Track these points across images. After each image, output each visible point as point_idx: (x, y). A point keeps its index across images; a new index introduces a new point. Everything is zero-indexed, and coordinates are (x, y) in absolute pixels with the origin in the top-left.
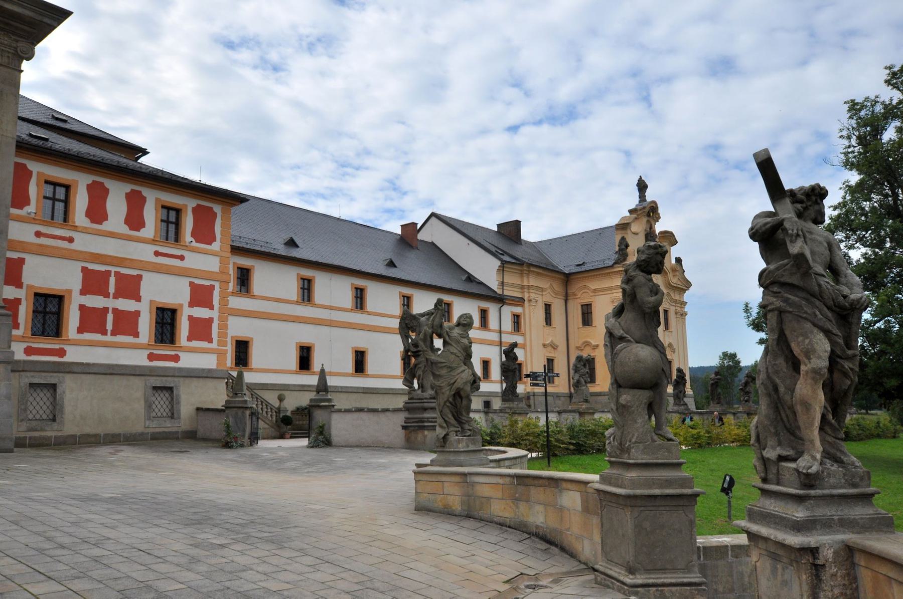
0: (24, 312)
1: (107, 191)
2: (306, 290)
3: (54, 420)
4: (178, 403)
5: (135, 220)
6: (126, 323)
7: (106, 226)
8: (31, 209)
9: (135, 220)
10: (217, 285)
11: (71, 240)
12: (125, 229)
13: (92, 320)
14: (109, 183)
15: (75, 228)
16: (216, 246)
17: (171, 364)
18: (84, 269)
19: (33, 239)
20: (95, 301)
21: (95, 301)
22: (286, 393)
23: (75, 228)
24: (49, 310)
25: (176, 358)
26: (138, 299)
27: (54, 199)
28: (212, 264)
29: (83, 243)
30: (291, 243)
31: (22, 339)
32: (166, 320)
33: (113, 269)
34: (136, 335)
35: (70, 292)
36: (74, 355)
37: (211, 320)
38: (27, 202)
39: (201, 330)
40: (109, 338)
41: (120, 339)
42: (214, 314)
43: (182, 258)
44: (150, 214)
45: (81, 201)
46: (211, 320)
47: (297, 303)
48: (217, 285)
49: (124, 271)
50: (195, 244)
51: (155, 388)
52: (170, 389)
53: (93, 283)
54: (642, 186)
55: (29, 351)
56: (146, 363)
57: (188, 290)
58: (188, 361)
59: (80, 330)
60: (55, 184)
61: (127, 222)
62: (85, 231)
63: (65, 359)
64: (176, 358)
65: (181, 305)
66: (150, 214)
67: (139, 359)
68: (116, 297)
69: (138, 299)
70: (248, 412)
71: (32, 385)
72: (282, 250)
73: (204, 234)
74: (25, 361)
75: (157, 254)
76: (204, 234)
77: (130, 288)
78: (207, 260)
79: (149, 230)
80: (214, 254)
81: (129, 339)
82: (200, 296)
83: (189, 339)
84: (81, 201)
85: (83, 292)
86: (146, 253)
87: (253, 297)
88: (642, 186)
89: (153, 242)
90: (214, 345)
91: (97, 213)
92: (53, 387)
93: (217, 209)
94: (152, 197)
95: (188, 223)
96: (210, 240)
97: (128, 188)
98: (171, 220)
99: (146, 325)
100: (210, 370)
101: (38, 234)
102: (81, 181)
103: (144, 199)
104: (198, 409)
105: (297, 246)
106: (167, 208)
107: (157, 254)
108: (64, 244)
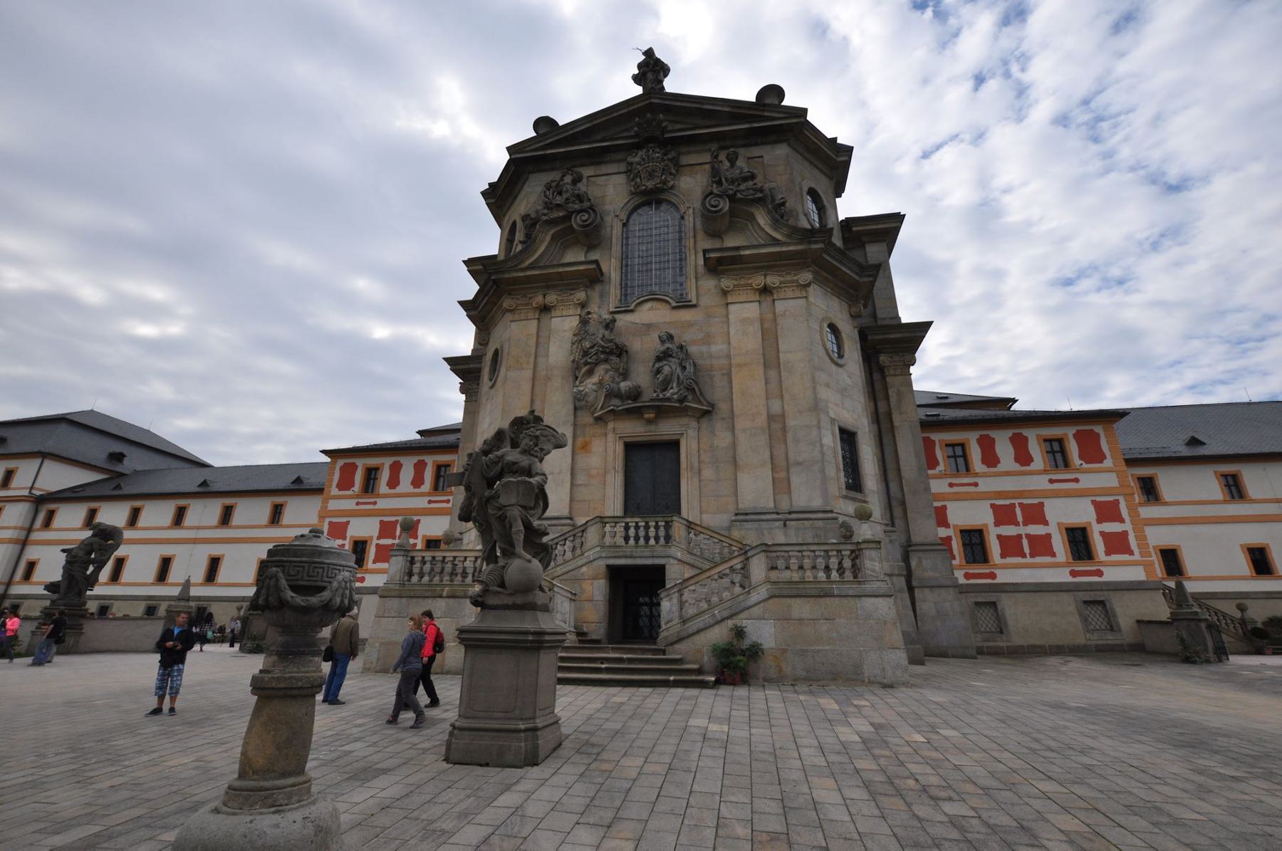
0: (956, 546)
1: (993, 440)
2: (1235, 489)
3: (1001, 632)
4: (1115, 616)
5: (1023, 457)
6: (1041, 546)
7: (1001, 467)
8: (941, 467)
9: (1023, 457)
10: (1121, 499)
11: (976, 485)
12: (1017, 467)
13: (1011, 546)
14: (994, 434)
15: (977, 475)
16: (1108, 463)
17: (1096, 579)
18: (993, 506)
19: (948, 490)
22: (1248, 602)
23: (977, 475)
24: (974, 541)
25: (1100, 573)
26: (1046, 523)
27: (955, 457)
28: (1111, 481)
29: (986, 485)
30: (1194, 442)
31: (960, 567)
32: (1078, 540)
33: (1016, 502)
34: (1053, 555)
35: (986, 525)
36: (1003, 577)
37: (1125, 534)
38: (938, 464)
39: (1117, 544)
40: (1029, 560)
41: (1039, 560)
42: (1127, 526)
43: (1076, 480)
45: (975, 453)
46: (1125, 534)
47: (1225, 502)
48: (1121, 499)
49: (1026, 501)
50: (1085, 466)
51: (1085, 602)
52: (1102, 603)
53: (1003, 515)
55: (967, 576)
56: (1070, 579)
57: (1091, 509)
58: (1112, 575)
59: (1003, 556)
60: (953, 445)
61: (1017, 460)
62: (985, 475)
63: (999, 580)
64: (1100, 573)
65: (1089, 523)
66: (1035, 449)
68: (1025, 524)
69: (1046, 523)
70: (1203, 625)
71: (977, 604)
72: (1185, 451)
73: (1092, 453)
74: (967, 585)
75: (1051, 481)
76: (1092, 453)
77: (1036, 515)
78: (1104, 478)
79: (1039, 461)
80: (1108, 471)
81: (1048, 559)
82: (1107, 512)
83: (1108, 553)
84: (975, 453)
85: (997, 524)
86: (1041, 482)
87: (1166, 504)
89: (1045, 472)
90: (1137, 557)
91: (990, 459)
92: (994, 604)
93: (1098, 429)
94: (1033, 437)
95: (1073, 448)
96: (1101, 458)
97: (1009, 433)
98: (1057, 451)
99: (1060, 545)
100: (1140, 582)
101: (951, 485)
102: (972, 439)
103: (1026, 439)
104: (1138, 622)
105: (1203, 444)
106: (1048, 441)
107: (1051, 481)
108: (972, 489)
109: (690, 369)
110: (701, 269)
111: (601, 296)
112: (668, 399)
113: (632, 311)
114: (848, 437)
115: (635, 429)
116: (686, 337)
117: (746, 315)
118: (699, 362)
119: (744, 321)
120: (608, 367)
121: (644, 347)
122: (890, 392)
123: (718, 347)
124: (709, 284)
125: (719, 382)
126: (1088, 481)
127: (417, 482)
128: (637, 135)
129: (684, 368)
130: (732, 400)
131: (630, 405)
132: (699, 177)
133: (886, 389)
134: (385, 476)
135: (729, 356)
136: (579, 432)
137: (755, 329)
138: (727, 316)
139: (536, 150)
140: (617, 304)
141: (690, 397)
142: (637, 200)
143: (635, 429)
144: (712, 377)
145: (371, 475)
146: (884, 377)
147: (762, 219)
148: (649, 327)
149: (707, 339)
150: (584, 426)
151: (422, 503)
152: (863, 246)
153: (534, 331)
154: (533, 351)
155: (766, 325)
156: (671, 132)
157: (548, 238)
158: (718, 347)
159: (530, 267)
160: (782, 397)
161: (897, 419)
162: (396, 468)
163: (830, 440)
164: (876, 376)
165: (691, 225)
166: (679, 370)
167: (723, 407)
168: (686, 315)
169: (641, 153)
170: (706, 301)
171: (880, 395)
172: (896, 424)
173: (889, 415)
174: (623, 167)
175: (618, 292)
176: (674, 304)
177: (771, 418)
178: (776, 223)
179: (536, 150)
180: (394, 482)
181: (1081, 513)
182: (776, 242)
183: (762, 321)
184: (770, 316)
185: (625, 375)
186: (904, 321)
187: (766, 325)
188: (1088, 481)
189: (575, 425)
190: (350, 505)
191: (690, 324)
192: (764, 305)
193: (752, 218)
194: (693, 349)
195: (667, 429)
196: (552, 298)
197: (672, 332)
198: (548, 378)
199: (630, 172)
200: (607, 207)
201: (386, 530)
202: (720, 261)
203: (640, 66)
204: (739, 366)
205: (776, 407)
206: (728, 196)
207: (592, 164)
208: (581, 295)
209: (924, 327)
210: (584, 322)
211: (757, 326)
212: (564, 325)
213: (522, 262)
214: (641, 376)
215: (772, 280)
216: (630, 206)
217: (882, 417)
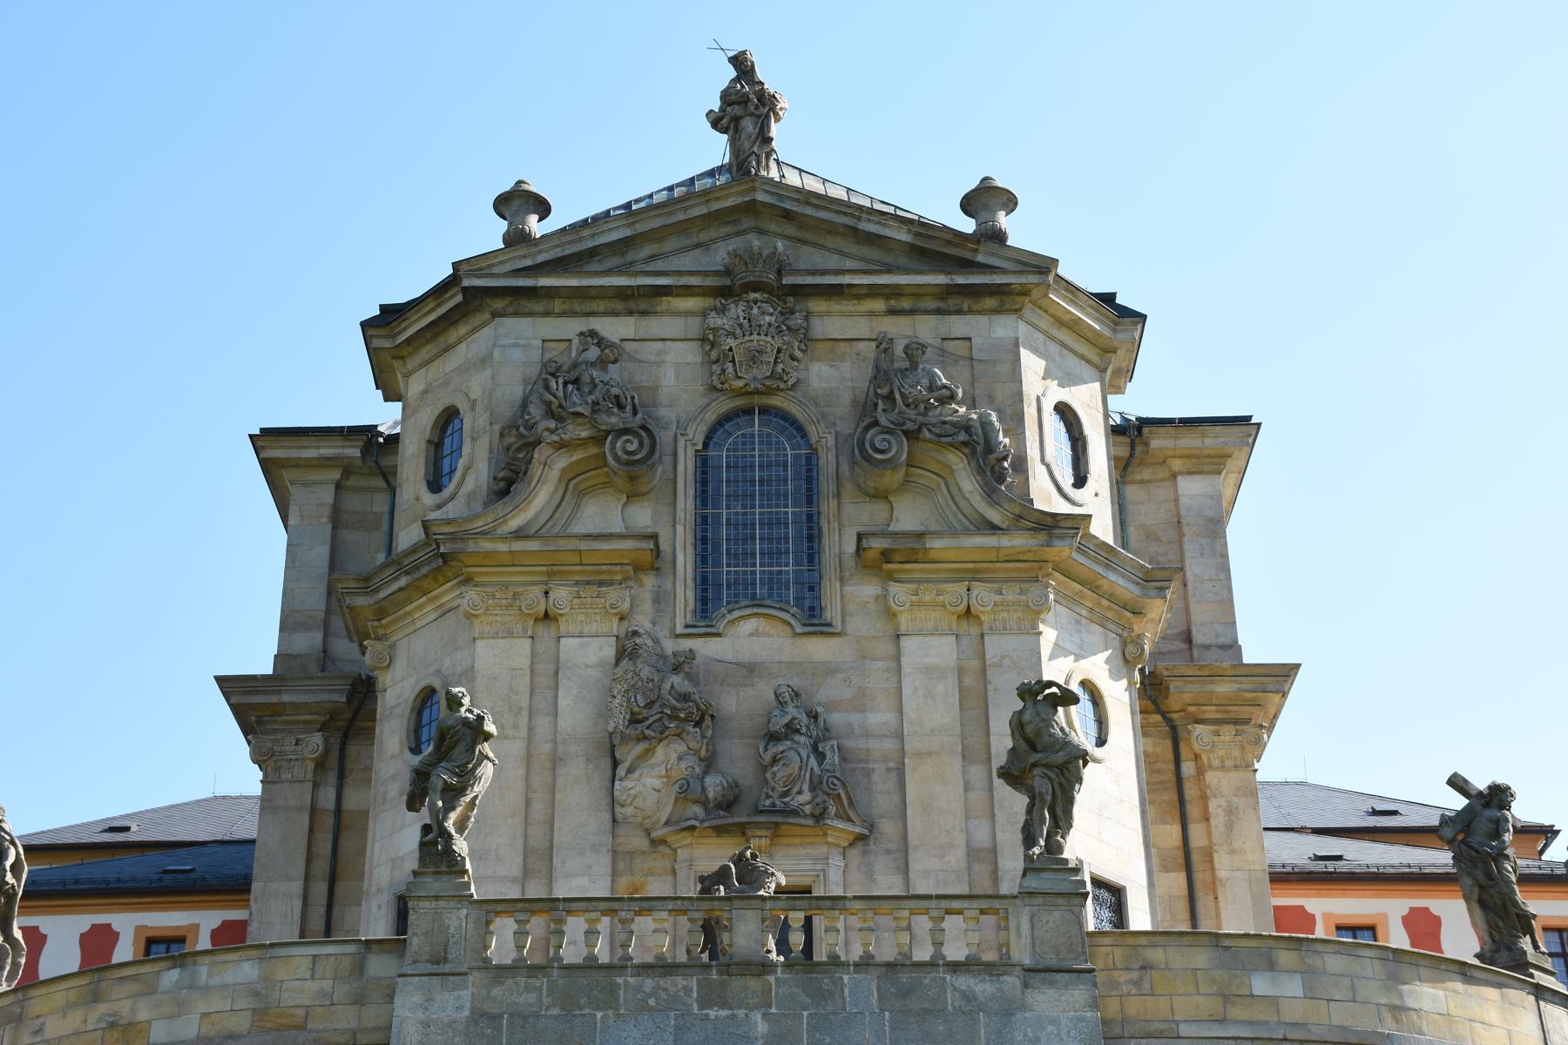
1: (1436, 922)
109: (832, 758)
110: (849, 562)
111: (656, 601)
112: (794, 813)
113: (718, 635)
116: (827, 692)
117: (931, 661)
118: (849, 743)
119: (928, 671)
120: (682, 748)
121: (739, 704)
122: (1213, 805)
123: (880, 718)
124: (865, 590)
125: (882, 782)
128: (727, 272)
129: (821, 757)
130: (904, 817)
132: (846, 367)
133: (1204, 798)
135: (899, 735)
136: (621, 866)
137: (947, 689)
138: (898, 658)
139: (516, 272)
140: (689, 619)
141: (833, 810)
142: (724, 405)
144: (868, 774)
146: (1200, 772)
147: (968, 484)
148: (751, 670)
149: (860, 702)
150: (631, 854)
152: (1174, 476)
153: (525, 662)
154: (525, 704)
155: (968, 681)
156: (798, 272)
157: (554, 474)
158: (880, 718)
159: (519, 534)
160: (993, 816)
161: (1224, 864)
164: (1188, 768)
165: (832, 469)
166: (813, 761)
167: (888, 828)
168: (819, 649)
169: (737, 310)
170: (859, 625)
171: (1193, 811)
172: (1222, 873)
173: (1209, 855)
174: (694, 326)
175: (690, 594)
176: (799, 630)
177: (972, 853)
178: (991, 494)
179: (516, 272)
182: (993, 528)
183: (961, 671)
184: (975, 663)
185: (709, 763)
186: (1245, 661)
187: (968, 681)
189: (614, 852)
191: (829, 670)
192: (965, 641)
193: (946, 475)
194: (836, 719)
196: (562, 594)
197: (796, 682)
198: (556, 761)
199: (707, 340)
200: (662, 412)
202: (886, 555)
203: (726, 96)
204: (918, 754)
205: (981, 836)
206: (907, 433)
207: (630, 313)
208: (617, 596)
209: (1285, 674)
210: (626, 650)
211: (952, 680)
212: (587, 650)
213: (504, 519)
214: (738, 760)
215: (983, 596)
216: (711, 416)
217: (1196, 858)
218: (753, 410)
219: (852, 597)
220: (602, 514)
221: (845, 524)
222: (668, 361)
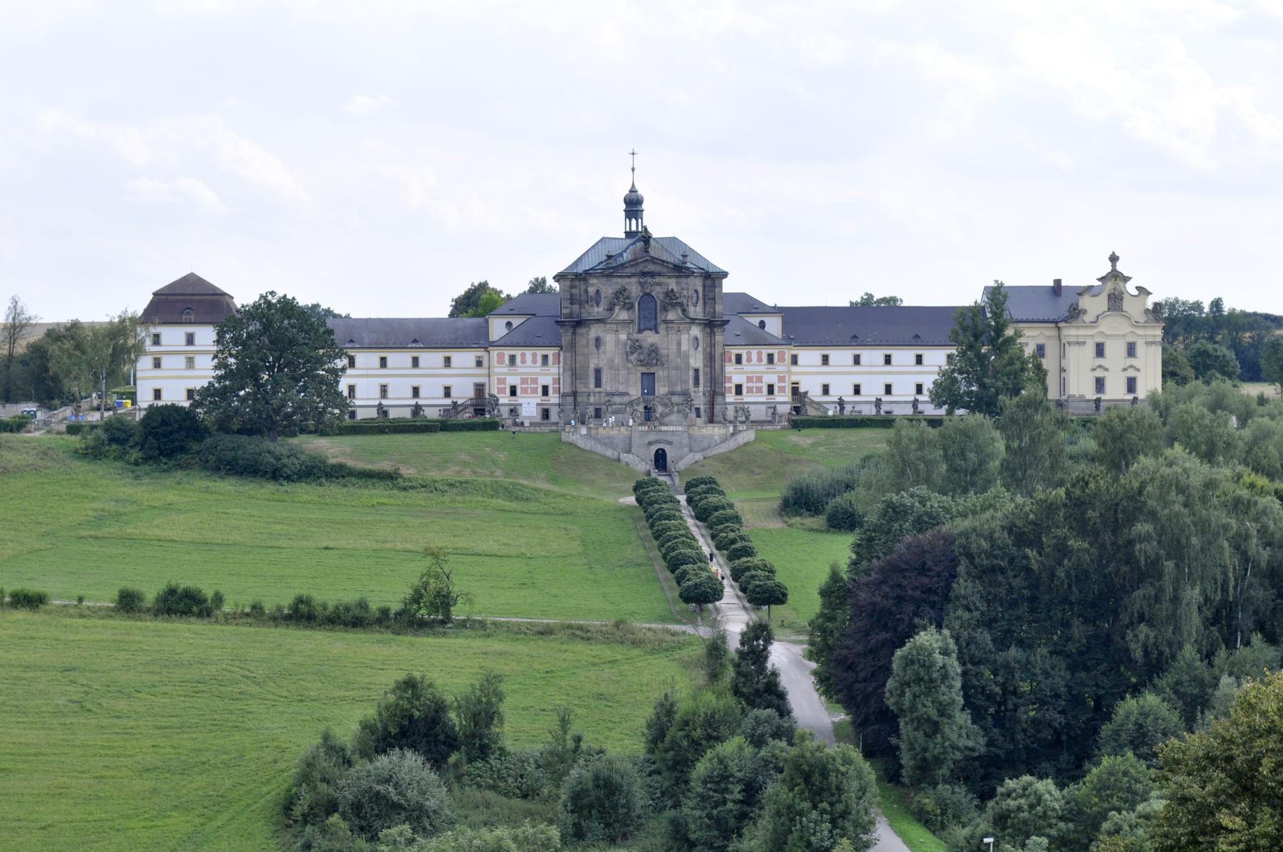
6: (759, 390)
13: (750, 390)
20: (750, 385)
21: (750, 385)
29: (747, 368)
32: (771, 389)
39: (782, 390)
44: (765, 358)
53: (749, 380)
54: (1114, 259)
58: (778, 399)
67: (763, 399)
77: (760, 380)
82: (781, 379)
84: (744, 358)
86: (763, 368)
88: (1114, 259)
99: (765, 390)
114: (697, 371)
115: (644, 370)
126: (779, 368)
127: (534, 361)
131: (641, 362)
134: (518, 359)
143: (644, 370)
145: (512, 358)
147: (679, 311)
151: (538, 370)
162: (523, 355)
163: (691, 373)
180: (523, 361)
181: (772, 379)
188: (779, 368)
190: (505, 370)
195: (652, 371)
201: (524, 381)
212: (623, 337)
218: (647, 295)
219: (662, 328)
220: (624, 315)
221: (660, 317)
222: (634, 289)
